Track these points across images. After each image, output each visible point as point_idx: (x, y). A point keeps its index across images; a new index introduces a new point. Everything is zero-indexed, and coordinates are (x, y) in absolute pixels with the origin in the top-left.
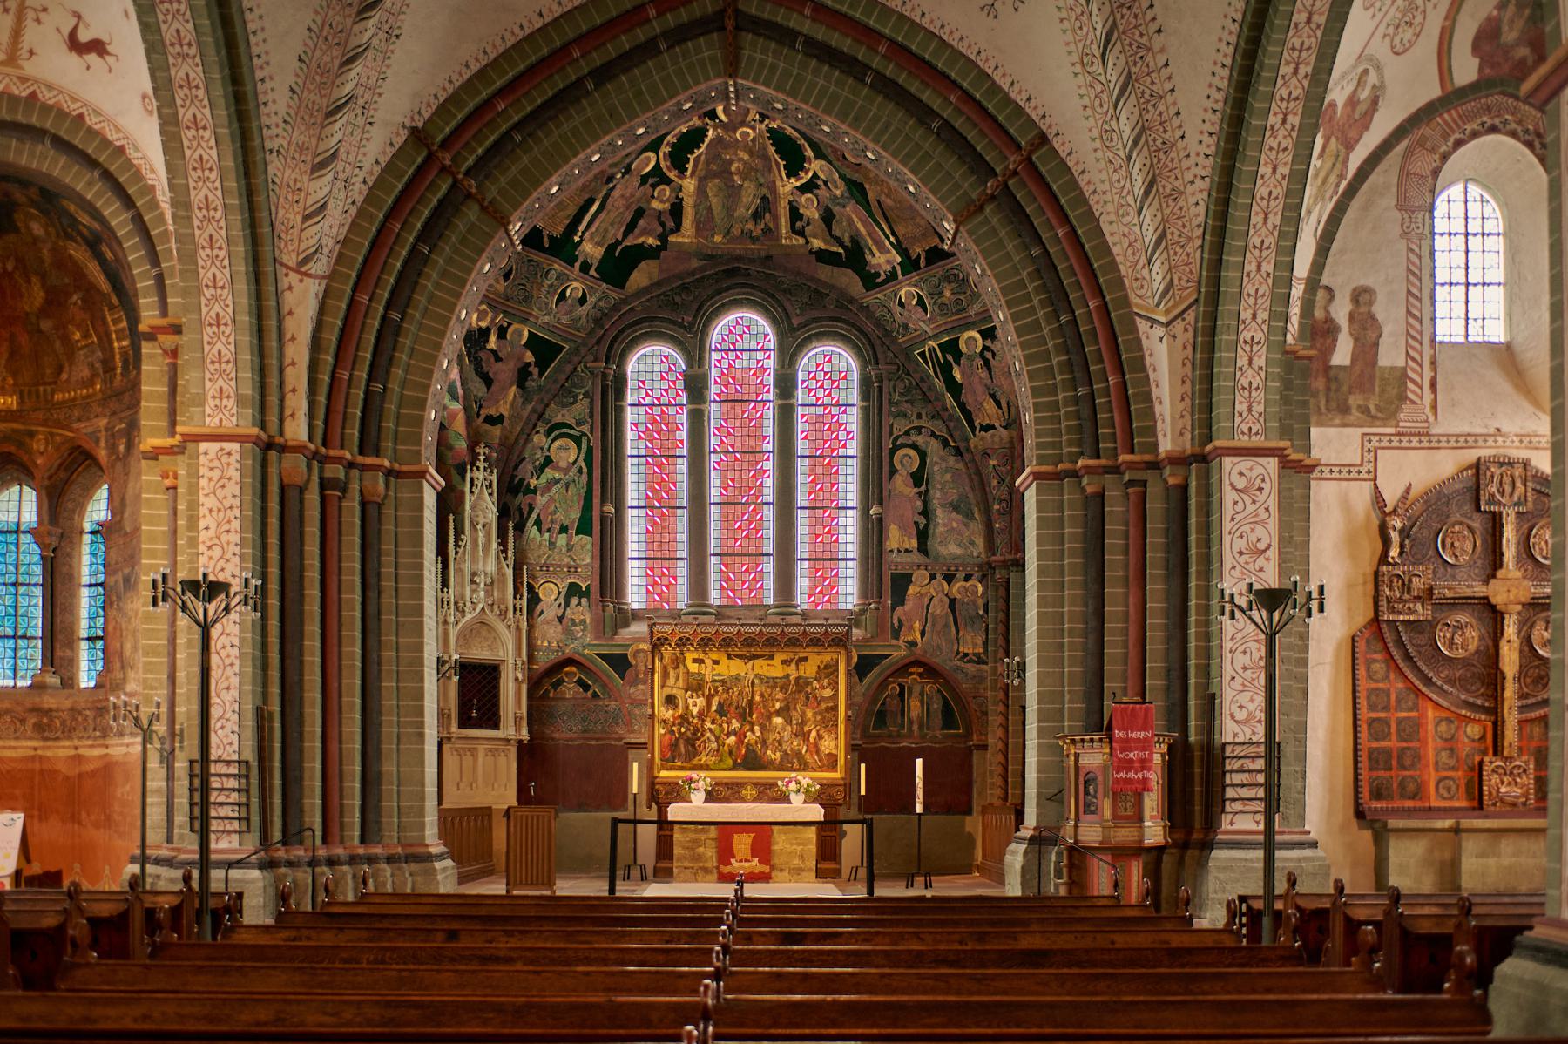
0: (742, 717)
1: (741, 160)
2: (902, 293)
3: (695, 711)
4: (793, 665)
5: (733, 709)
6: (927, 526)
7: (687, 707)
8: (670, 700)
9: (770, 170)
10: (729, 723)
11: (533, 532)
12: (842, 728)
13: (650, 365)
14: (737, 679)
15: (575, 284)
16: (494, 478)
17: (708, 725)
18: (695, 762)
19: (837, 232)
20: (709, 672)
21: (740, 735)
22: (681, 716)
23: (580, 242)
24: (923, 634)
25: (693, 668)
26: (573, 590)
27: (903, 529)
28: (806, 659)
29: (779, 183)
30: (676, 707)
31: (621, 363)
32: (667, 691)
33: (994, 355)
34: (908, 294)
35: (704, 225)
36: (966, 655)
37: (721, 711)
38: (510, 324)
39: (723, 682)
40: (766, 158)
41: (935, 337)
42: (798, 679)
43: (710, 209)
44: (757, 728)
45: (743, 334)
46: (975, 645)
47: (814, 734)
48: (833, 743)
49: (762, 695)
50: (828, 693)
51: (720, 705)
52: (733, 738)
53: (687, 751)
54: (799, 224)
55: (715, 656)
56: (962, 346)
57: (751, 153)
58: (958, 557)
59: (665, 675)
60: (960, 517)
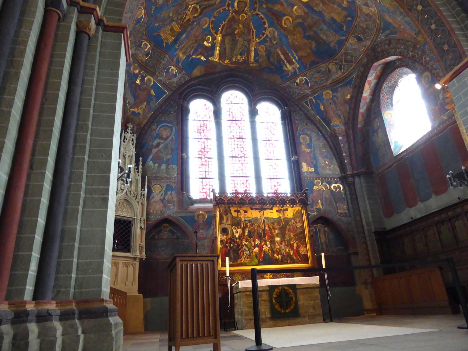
0: (260, 238)
1: (240, 28)
2: (298, 81)
3: (237, 235)
4: (282, 212)
5: (256, 233)
6: (316, 163)
7: (233, 233)
8: (224, 231)
9: (249, 33)
10: (254, 241)
11: (150, 163)
12: (308, 241)
13: (199, 108)
14: (256, 219)
15: (173, 68)
16: (135, 138)
17: (244, 242)
18: (239, 262)
19: (272, 60)
20: (242, 216)
21: (261, 247)
22: (230, 239)
23: (176, 50)
24: (322, 205)
25: (235, 214)
26: (169, 188)
27: (308, 165)
28: (287, 210)
29: (252, 41)
30: (227, 234)
31: (188, 103)
32: (223, 226)
33: (337, 98)
34: (301, 80)
35: (222, 55)
36: (341, 213)
37: (250, 235)
38: (146, 76)
39: (250, 221)
40: (249, 29)
41: (312, 95)
42: (284, 219)
43: (225, 49)
44: (268, 243)
45: (234, 100)
46: (344, 210)
47: (295, 245)
48: (305, 249)
49: (269, 227)
50: (299, 225)
51: (249, 232)
52: (257, 249)
53: (234, 256)
54: (257, 58)
55: (245, 209)
56: (324, 97)
57: (244, 26)
58: (330, 175)
59: (221, 219)
60: (328, 160)
